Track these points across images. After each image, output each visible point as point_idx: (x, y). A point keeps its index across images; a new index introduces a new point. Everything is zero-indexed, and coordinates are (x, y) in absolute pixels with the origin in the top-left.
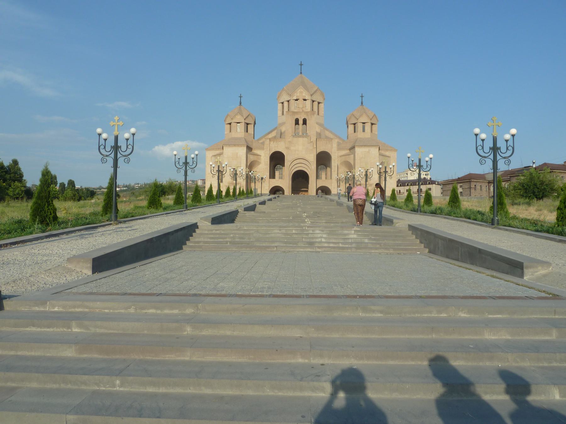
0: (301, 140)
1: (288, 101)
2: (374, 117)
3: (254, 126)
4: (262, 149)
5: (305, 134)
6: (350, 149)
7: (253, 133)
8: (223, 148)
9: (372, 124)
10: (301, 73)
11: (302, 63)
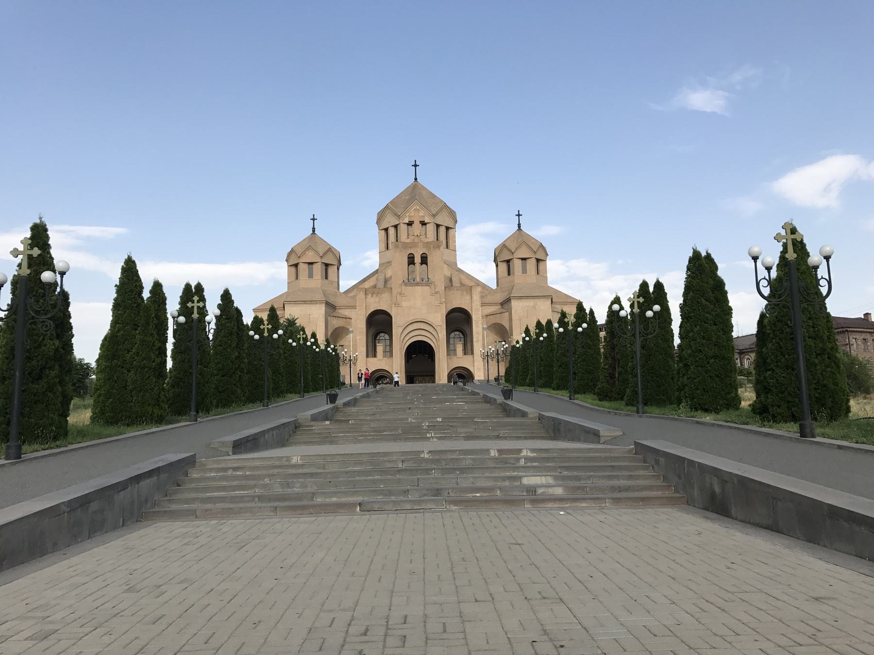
0: (420, 291)
1: (396, 227)
3: (338, 269)
4: (354, 307)
5: (426, 282)
6: (502, 304)
7: (336, 280)
8: (284, 307)
9: (538, 260)
10: (416, 179)
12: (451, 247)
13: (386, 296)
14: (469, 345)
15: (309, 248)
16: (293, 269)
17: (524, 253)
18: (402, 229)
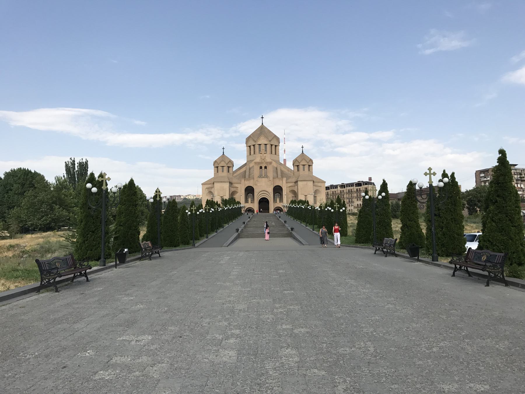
1: (254, 145)
2: (310, 161)
5: (266, 176)
8: (214, 183)
9: (309, 166)
10: (262, 124)
11: (263, 117)
12: (277, 154)
13: (252, 181)
14: (282, 198)
15: (223, 161)
16: (216, 168)
17: (303, 163)
18: (256, 147)
